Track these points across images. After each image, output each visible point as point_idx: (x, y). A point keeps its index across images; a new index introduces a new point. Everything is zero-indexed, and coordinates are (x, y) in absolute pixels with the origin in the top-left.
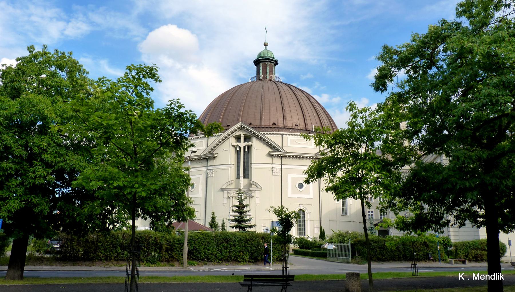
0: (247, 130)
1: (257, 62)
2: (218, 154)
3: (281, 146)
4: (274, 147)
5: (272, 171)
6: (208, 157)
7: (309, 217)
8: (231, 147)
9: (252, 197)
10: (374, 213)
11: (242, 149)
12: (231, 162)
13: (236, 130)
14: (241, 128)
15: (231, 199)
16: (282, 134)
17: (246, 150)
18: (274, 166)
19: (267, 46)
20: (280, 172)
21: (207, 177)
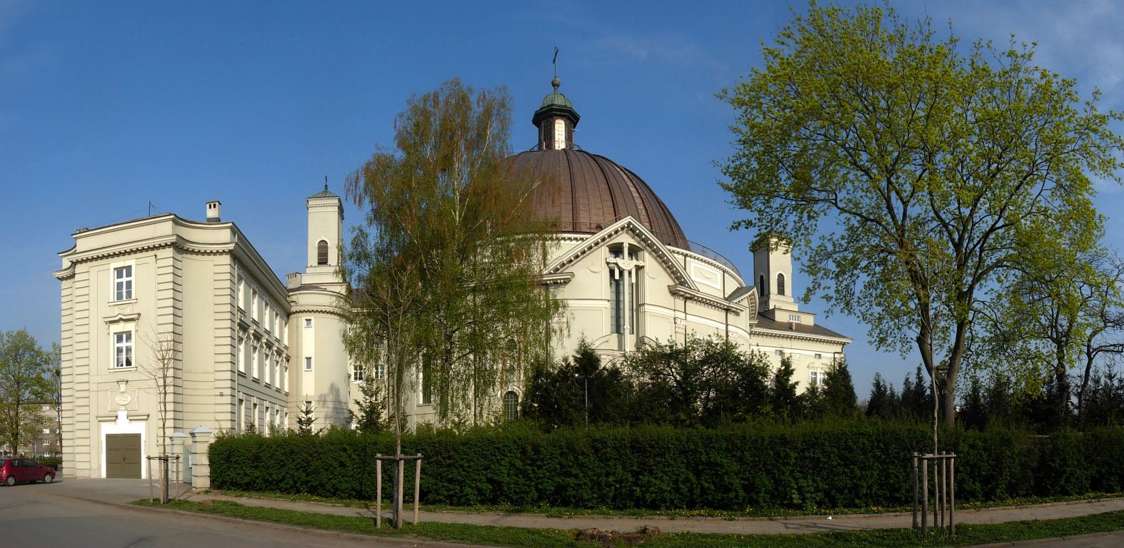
5: (675, 323)
6: (552, 280)
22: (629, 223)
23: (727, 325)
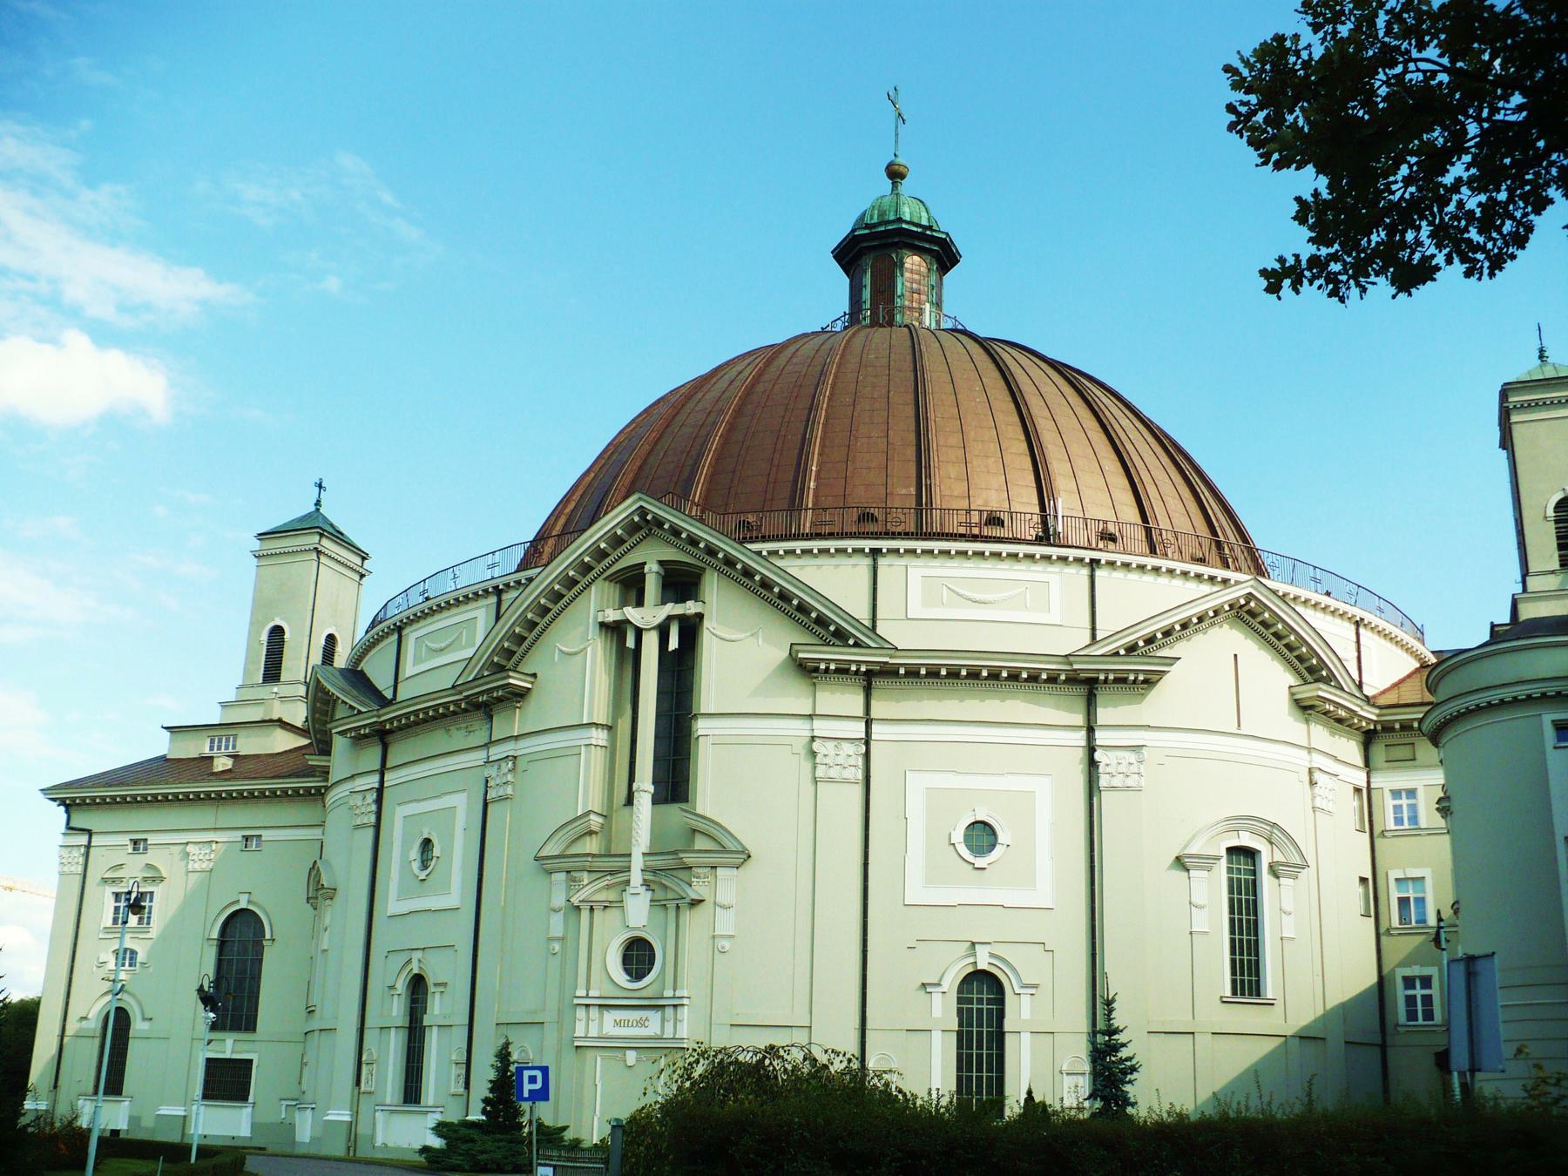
0: (676, 532)
1: (850, 254)
2: (534, 675)
3: (863, 615)
4: (822, 621)
5: (814, 754)
7: (1026, 1014)
8: (593, 632)
9: (695, 903)
10: (1435, 991)
11: (651, 643)
12: (591, 713)
13: (616, 541)
14: (644, 526)
15: (585, 914)
16: (876, 553)
17: (673, 644)
18: (821, 728)
19: (902, 176)
20: (860, 762)
21: (486, 805)
22: (642, 512)
23: (1091, 730)
